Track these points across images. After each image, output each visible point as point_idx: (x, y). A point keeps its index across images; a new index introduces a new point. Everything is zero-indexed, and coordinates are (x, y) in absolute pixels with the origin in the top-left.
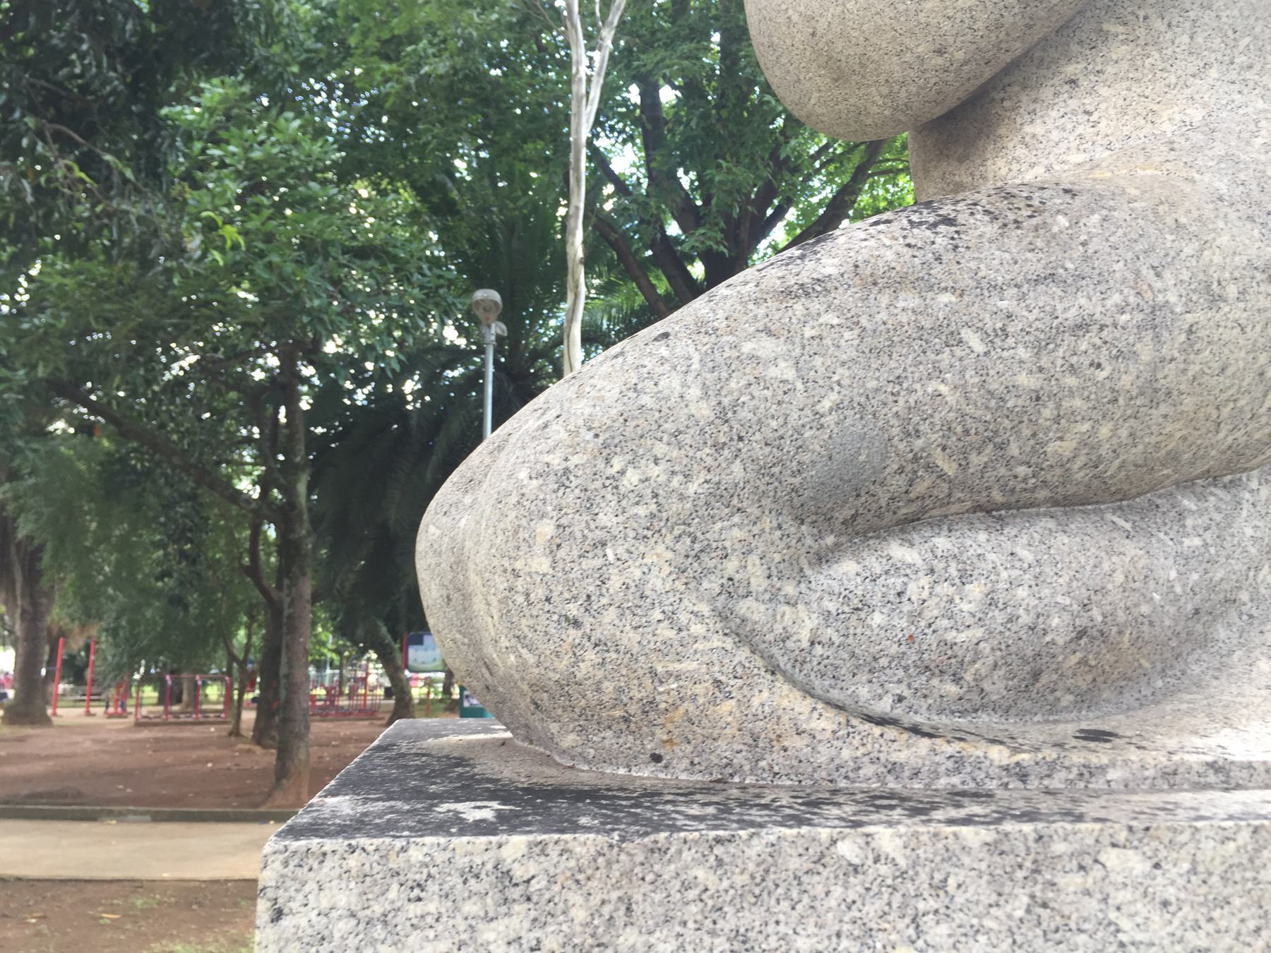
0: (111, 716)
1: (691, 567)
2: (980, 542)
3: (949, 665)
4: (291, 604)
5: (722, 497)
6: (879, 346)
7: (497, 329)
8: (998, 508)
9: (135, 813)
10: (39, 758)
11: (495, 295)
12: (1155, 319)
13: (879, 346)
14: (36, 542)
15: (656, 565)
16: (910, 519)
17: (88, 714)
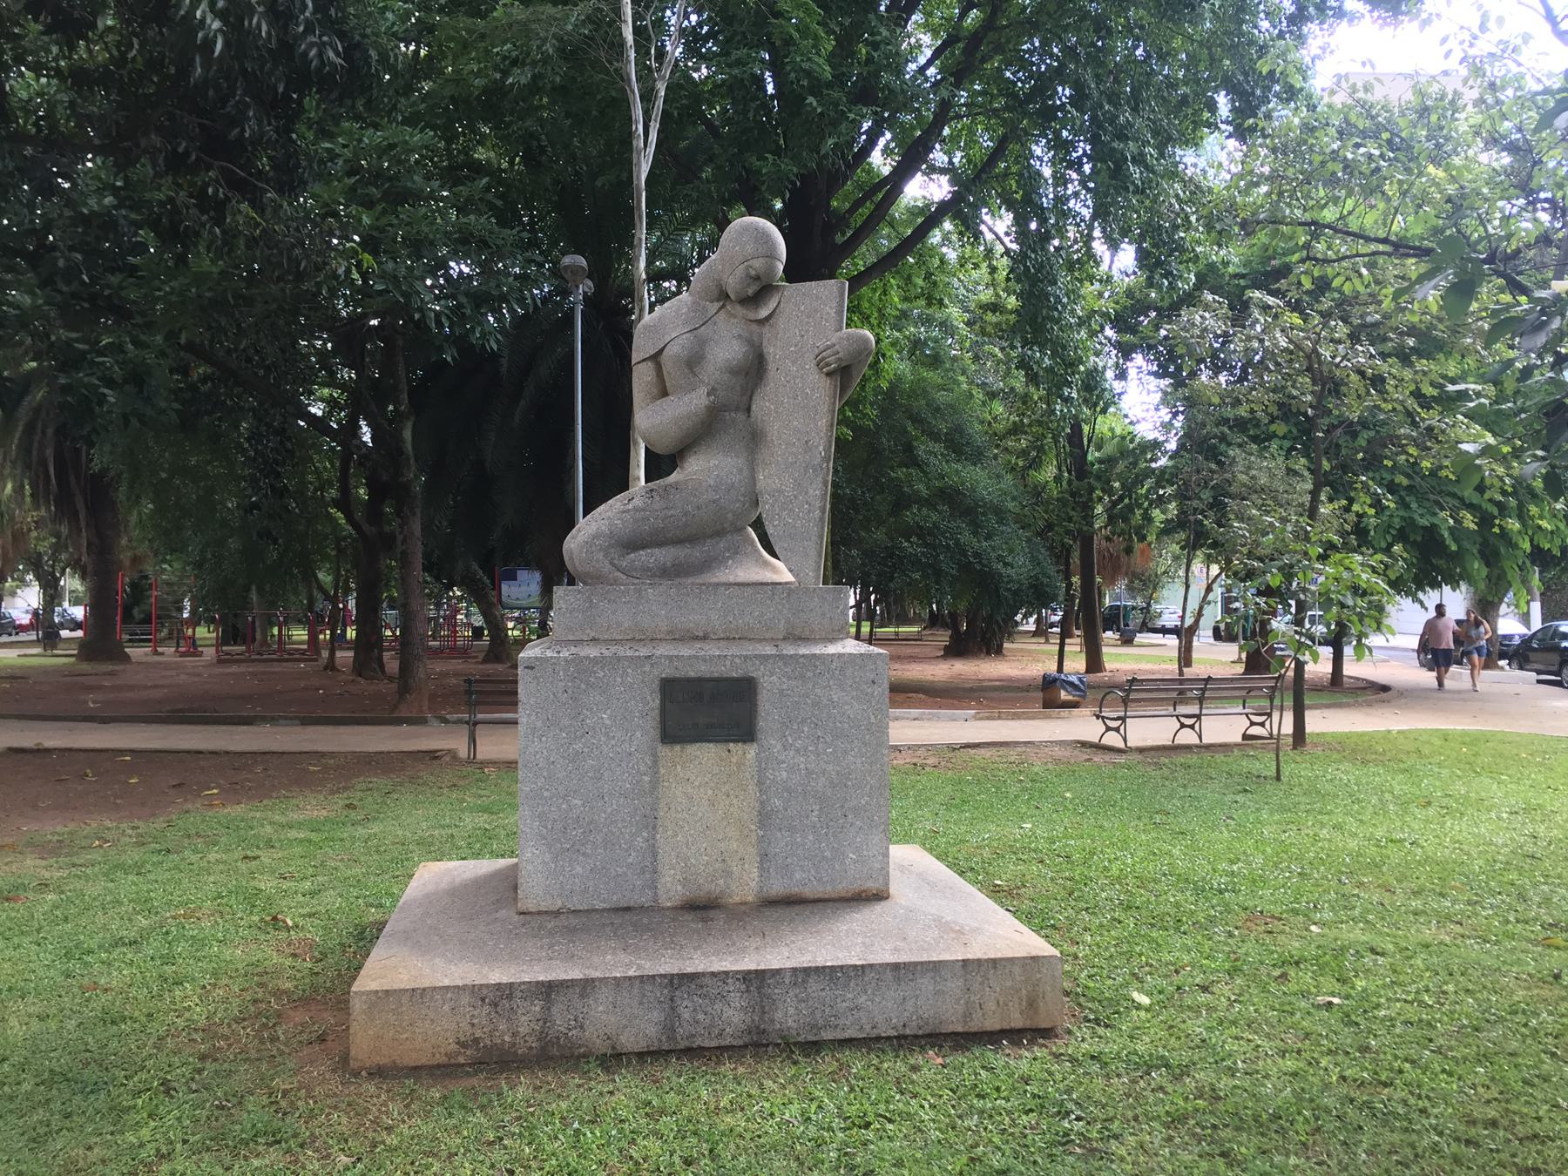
0: (183, 655)
1: (606, 556)
2: (656, 551)
3: (649, 570)
4: (404, 541)
5: (611, 546)
6: (636, 521)
7: (586, 287)
8: (660, 545)
9: (286, 718)
10: (146, 687)
11: (584, 262)
12: (686, 514)
13: (636, 521)
14: (112, 473)
15: (601, 556)
16: (643, 547)
17: (156, 653)
